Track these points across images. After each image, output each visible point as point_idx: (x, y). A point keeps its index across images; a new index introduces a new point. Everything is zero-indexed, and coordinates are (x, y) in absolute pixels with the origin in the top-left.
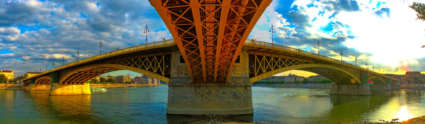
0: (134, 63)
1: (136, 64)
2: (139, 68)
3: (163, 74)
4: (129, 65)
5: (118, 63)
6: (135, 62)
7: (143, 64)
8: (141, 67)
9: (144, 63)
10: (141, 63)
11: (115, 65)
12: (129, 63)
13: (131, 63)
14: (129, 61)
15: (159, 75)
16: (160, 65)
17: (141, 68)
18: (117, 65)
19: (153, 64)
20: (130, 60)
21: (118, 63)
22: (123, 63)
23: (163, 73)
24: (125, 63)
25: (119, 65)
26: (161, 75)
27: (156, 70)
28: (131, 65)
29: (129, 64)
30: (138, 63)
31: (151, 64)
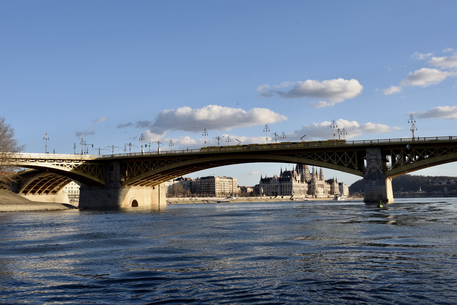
3: (357, 168)
4: (320, 160)
6: (339, 157)
13: (333, 158)
26: (354, 169)
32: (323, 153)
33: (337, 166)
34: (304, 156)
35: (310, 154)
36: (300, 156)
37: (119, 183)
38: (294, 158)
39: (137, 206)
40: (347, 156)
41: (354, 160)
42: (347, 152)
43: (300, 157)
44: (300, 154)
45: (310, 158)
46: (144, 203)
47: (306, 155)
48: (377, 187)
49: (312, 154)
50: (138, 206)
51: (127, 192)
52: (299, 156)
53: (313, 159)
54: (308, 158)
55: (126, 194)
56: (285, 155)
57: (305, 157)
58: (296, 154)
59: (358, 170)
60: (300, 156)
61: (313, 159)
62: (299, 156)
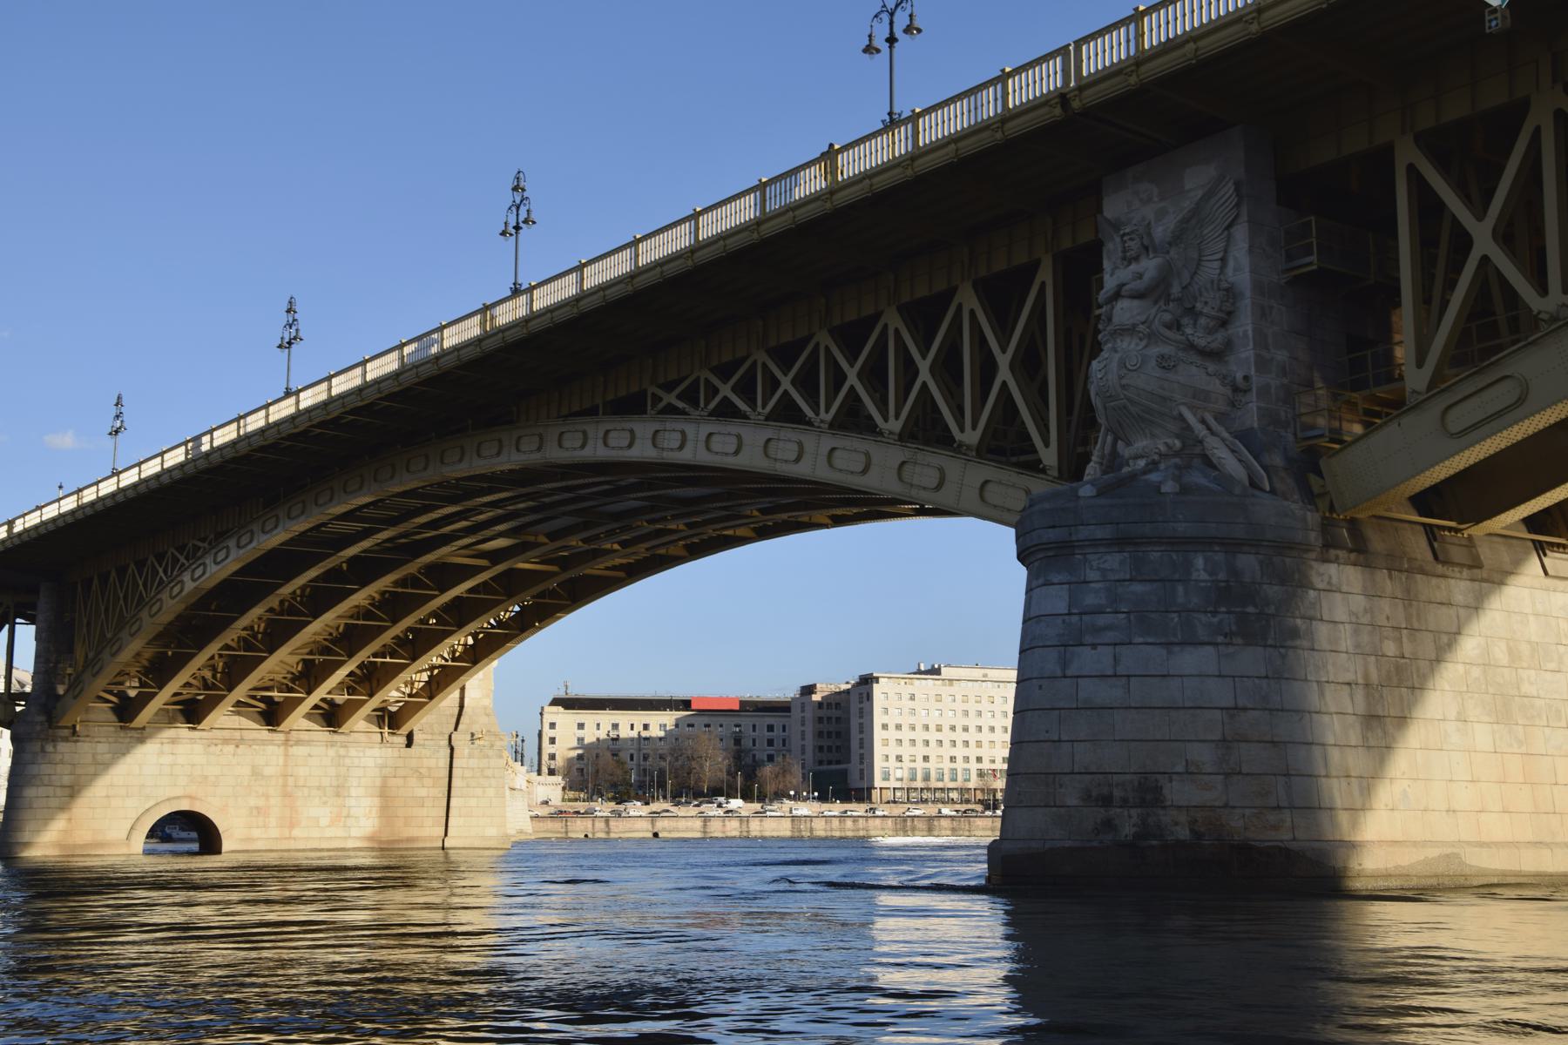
1: (786, 392)
2: (810, 423)
5: (680, 405)
7: (852, 379)
9: (859, 376)
10: (838, 378)
11: (644, 428)
16: (1012, 367)
17: (838, 425)
19: (948, 368)
21: (680, 405)
28: (742, 406)
31: (924, 375)
34: (691, 397)
43: (671, 410)
46: (296, 832)
48: (1088, 659)
56: (591, 412)
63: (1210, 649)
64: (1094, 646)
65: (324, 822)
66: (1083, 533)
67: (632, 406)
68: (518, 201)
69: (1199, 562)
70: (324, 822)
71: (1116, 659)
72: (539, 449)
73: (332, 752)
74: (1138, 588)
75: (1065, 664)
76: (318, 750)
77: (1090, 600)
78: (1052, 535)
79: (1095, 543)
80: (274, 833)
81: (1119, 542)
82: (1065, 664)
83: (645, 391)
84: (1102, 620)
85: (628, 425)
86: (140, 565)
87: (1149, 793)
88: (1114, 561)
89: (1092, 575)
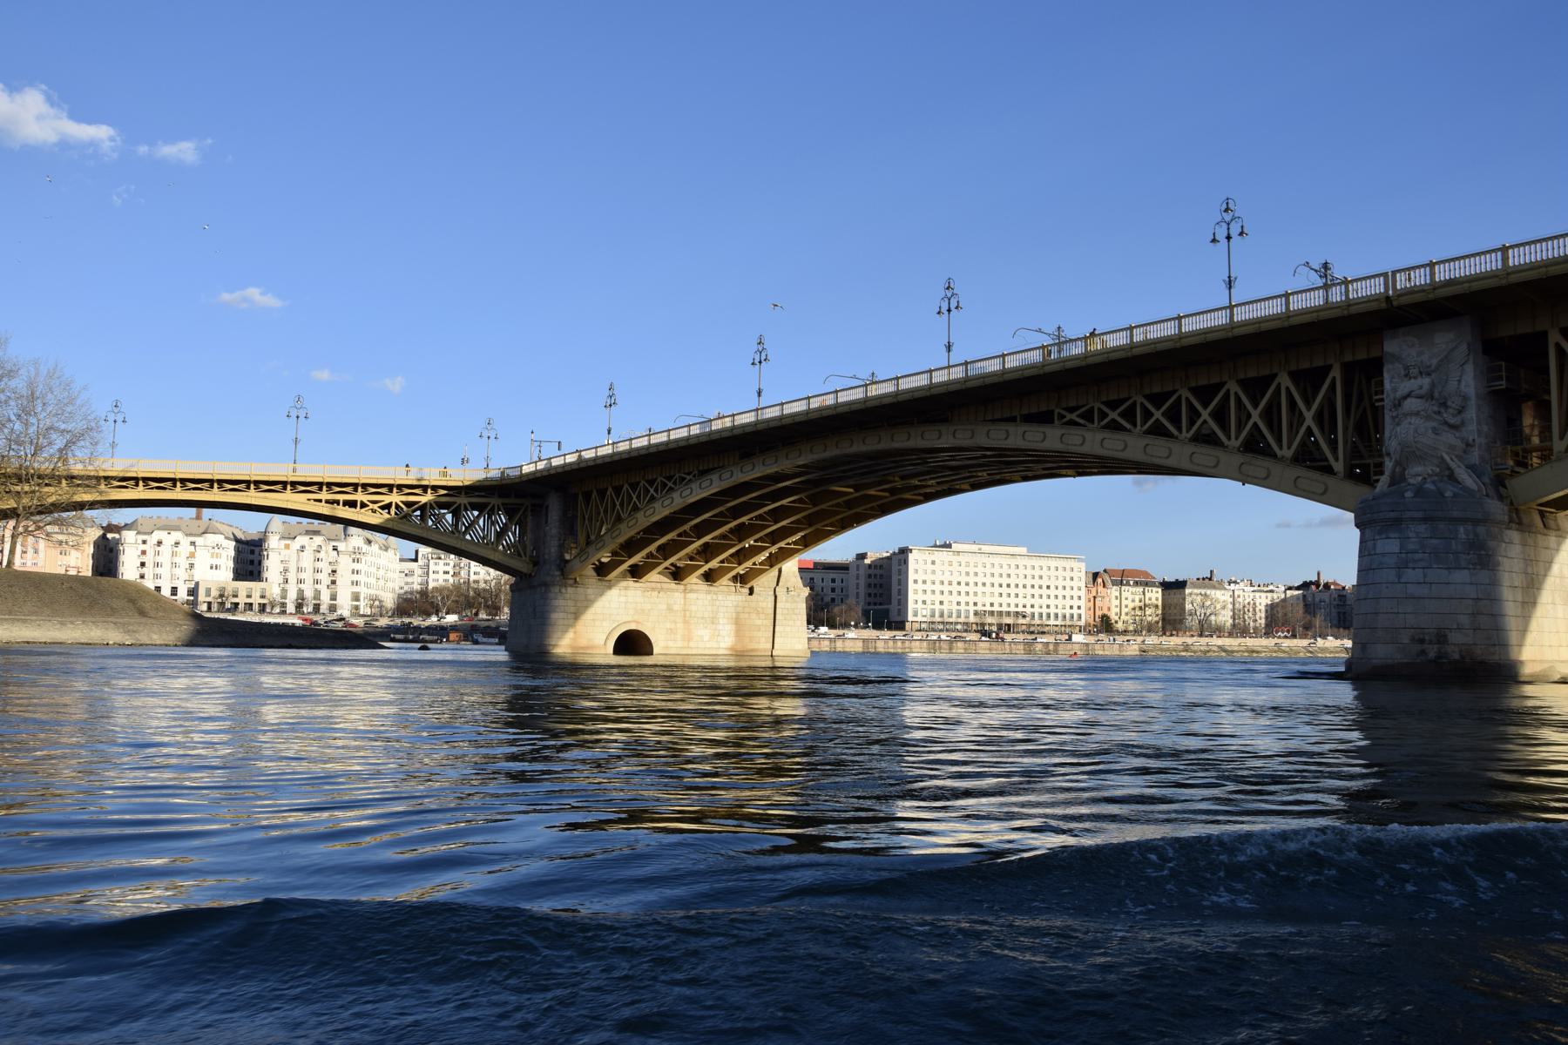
0: (1194, 415)
3: (1339, 466)
8: (1192, 432)
12: (1158, 415)
14: (1158, 400)
15: (1316, 475)
18: (1073, 430)
20: (1165, 396)
22: (1113, 415)
23: (1337, 459)
24: (1129, 415)
25: (1088, 435)
26: (1329, 470)
27: (1289, 448)
29: (1157, 420)
30: (1220, 416)
32: (1175, 391)
33: (1238, 459)
35: (1113, 405)
36: (1073, 416)
37: (553, 567)
38: (1048, 430)
39: (651, 653)
40: (1239, 400)
41: (1326, 419)
42: (1294, 376)
44: (1071, 410)
45: (1114, 427)
47: (1099, 409)
48: (1411, 575)
49: (1123, 401)
50: (652, 654)
51: (588, 603)
52: (1069, 416)
53: (1125, 429)
54: (1106, 427)
55: (587, 607)
56: (1012, 420)
57: (1093, 422)
58: (1057, 411)
59: (1350, 475)
60: (1073, 416)
61: (1125, 429)
62: (1069, 416)
63: (1466, 571)
64: (1414, 568)
65: (706, 638)
66: (1409, 514)
67: (1045, 418)
68: (949, 295)
69: (1462, 530)
70: (706, 638)
71: (1425, 576)
72: (972, 437)
73: (709, 597)
74: (1434, 541)
75: (1399, 577)
76: (702, 596)
77: (1411, 547)
78: (1392, 515)
79: (1413, 519)
80: (680, 644)
81: (1425, 520)
82: (1399, 577)
83: (1053, 411)
84: (1417, 556)
85: (1041, 429)
86: (618, 490)
87: (1441, 638)
88: (1422, 528)
89: (1411, 535)
